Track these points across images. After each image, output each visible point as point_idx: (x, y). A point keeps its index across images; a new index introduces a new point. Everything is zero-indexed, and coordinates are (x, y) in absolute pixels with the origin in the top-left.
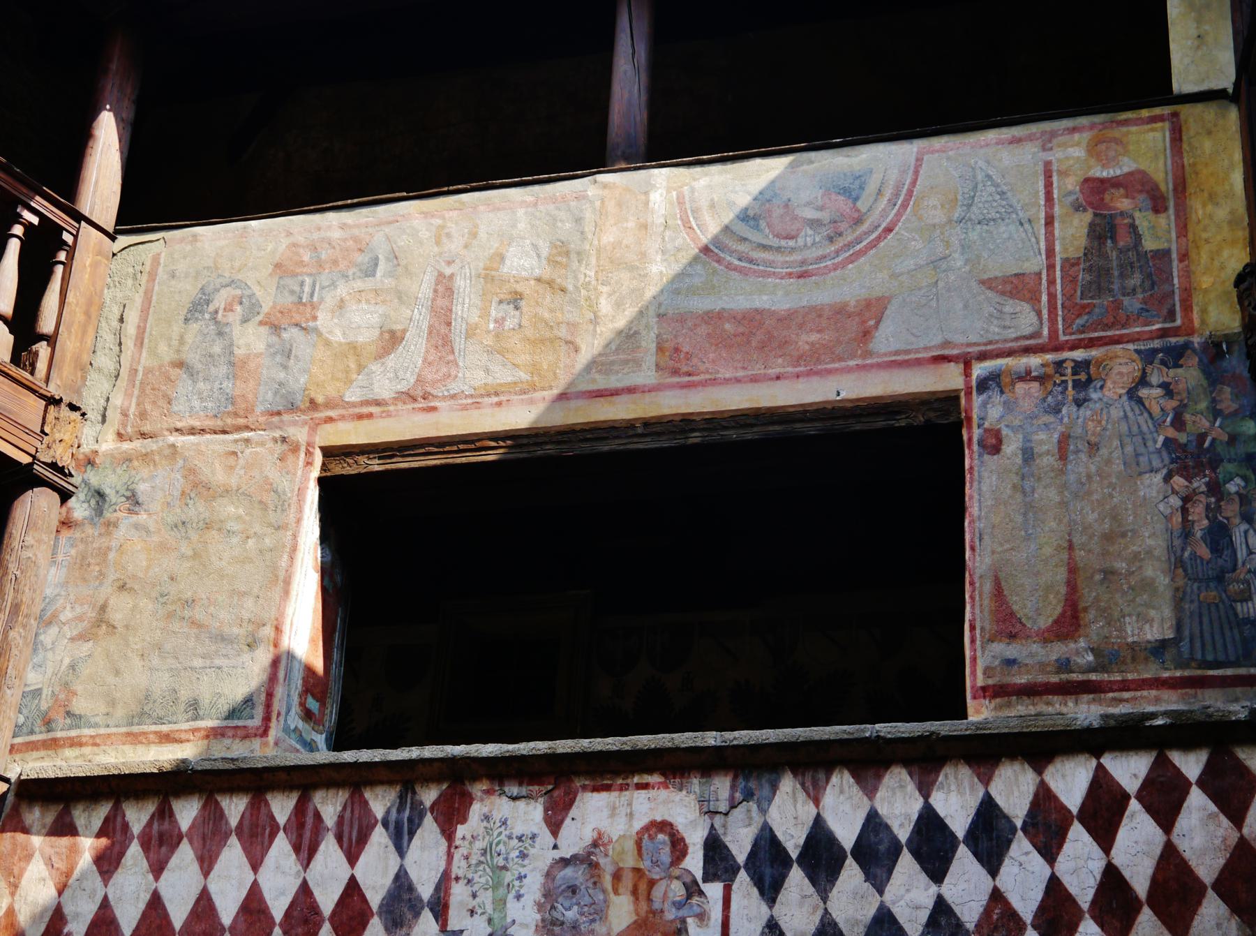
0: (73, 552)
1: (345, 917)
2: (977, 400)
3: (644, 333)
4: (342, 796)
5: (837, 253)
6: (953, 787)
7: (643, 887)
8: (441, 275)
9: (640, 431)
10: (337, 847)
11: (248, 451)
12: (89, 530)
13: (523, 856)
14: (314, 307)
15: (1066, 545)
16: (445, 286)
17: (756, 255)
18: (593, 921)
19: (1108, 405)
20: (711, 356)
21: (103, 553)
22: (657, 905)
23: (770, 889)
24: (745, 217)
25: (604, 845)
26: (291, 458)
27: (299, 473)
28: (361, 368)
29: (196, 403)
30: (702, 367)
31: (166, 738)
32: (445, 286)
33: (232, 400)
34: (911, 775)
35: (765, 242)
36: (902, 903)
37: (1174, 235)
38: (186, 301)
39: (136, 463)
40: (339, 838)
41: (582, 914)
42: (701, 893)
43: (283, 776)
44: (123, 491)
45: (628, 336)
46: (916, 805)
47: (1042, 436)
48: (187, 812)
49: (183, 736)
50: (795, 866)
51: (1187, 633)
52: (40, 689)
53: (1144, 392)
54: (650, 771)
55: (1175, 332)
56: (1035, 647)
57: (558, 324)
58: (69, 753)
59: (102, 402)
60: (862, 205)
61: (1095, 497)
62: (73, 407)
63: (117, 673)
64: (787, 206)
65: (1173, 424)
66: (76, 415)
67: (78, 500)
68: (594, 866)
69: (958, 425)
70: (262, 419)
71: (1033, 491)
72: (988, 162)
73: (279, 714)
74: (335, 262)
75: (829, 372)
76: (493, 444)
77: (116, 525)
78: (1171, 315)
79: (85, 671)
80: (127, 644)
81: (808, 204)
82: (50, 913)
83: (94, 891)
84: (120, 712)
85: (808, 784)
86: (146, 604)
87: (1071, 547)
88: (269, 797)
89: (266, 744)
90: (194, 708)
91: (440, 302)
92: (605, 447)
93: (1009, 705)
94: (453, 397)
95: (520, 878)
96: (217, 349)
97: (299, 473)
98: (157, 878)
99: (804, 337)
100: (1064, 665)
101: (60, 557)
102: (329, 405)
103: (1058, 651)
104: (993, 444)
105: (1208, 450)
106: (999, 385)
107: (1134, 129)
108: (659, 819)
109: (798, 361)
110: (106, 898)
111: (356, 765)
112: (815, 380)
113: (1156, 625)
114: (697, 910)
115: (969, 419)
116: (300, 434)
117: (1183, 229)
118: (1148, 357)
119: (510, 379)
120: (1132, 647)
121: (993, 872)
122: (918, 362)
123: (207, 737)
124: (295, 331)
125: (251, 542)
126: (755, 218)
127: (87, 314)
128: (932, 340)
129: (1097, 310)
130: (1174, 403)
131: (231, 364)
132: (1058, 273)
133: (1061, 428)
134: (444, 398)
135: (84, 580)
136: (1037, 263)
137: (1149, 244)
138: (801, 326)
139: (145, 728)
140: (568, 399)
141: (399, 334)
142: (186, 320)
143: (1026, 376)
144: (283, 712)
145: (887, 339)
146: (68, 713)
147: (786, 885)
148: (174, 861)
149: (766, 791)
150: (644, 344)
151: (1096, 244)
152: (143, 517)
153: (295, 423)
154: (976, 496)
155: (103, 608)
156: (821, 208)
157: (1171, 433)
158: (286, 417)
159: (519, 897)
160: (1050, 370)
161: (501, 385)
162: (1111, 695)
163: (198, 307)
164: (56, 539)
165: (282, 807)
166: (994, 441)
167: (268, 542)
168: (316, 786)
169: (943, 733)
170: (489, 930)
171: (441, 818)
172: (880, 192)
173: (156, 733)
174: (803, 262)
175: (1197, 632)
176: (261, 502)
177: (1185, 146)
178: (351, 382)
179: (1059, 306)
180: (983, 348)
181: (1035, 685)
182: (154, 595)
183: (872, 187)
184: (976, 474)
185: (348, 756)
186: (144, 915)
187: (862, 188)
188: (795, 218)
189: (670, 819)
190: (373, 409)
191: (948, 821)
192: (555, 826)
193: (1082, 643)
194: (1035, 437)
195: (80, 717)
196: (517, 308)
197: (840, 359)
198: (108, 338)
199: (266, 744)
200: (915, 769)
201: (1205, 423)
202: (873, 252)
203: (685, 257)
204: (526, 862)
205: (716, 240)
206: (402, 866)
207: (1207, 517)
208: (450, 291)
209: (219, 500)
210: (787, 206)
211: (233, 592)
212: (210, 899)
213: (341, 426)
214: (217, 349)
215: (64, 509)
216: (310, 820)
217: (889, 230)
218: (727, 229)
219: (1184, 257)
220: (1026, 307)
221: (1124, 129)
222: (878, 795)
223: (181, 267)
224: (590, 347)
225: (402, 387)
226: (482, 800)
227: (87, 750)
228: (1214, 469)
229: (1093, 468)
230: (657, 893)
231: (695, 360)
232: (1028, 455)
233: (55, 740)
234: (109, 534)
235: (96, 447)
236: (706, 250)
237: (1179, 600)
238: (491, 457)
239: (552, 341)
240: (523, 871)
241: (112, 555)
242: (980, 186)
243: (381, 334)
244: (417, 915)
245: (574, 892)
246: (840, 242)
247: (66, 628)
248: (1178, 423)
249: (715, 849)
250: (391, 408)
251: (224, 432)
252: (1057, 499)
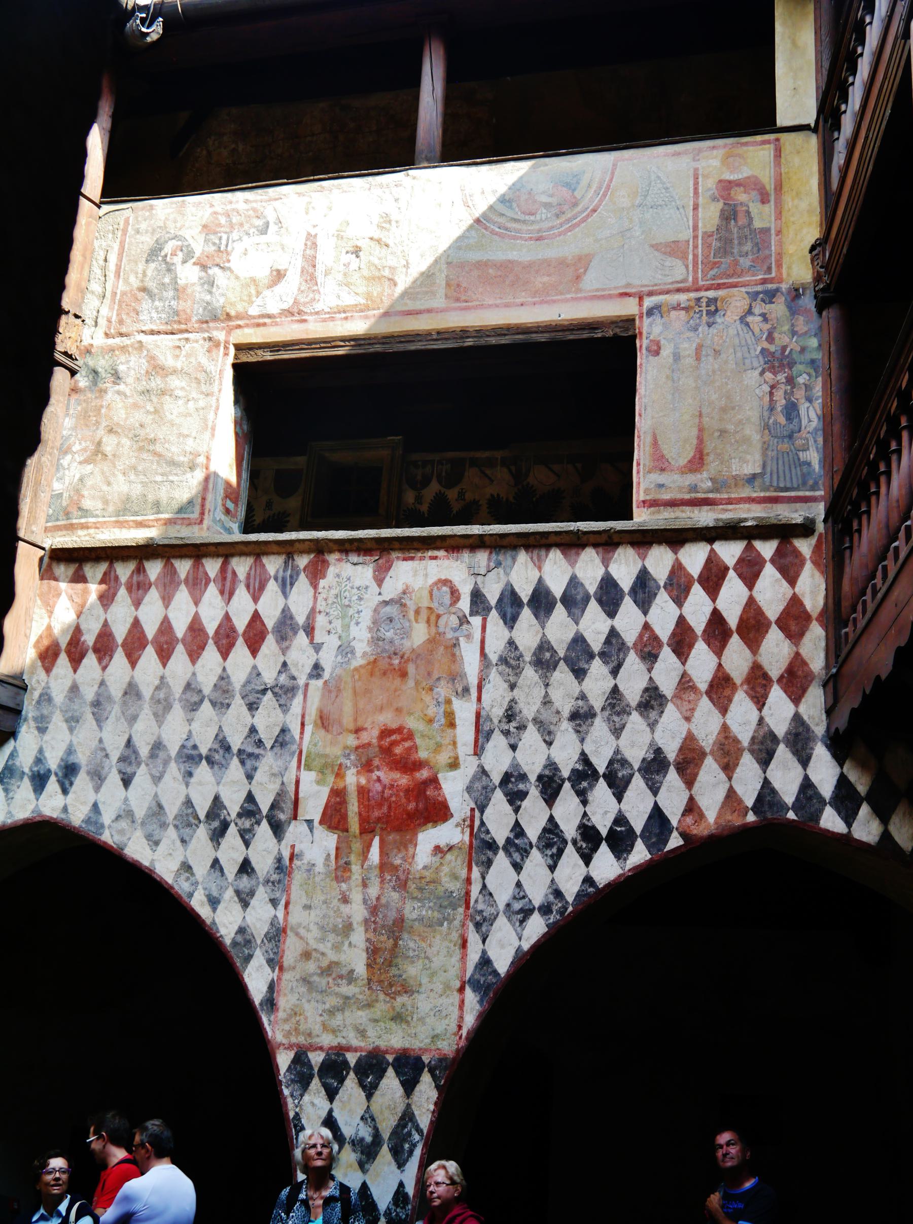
0: (79, 408)
1: (251, 634)
2: (646, 321)
3: (438, 274)
4: (249, 561)
5: (561, 225)
6: (623, 561)
7: (433, 618)
8: (309, 234)
9: (435, 337)
10: (246, 592)
11: (187, 346)
12: (89, 395)
13: (360, 599)
14: (228, 254)
15: (698, 414)
16: (312, 242)
17: (509, 225)
18: (403, 638)
19: (728, 327)
20: (480, 290)
21: (98, 409)
22: (441, 630)
23: (510, 621)
24: (503, 200)
25: (410, 593)
26: (214, 351)
27: (220, 360)
28: (258, 294)
29: (154, 315)
30: (474, 297)
31: (140, 525)
32: (312, 242)
33: (177, 313)
34: (597, 553)
35: (516, 217)
36: (590, 630)
37: (773, 218)
38: (146, 248)
39: (117, 353)
40: (248, 587)
41: (396, 634)
42: (468, 622)
43: (213, 549)
44: (109, 370)
45: (427, 277)
46: (600, 572)
47: (686, 345)
48: (154, 569)
49: (151, 523)
50: (526, 607)
51: (768, 470)
52: (62, 494)
53: (750, 319)
54: (438, 548)
55: (771, 281)
56: (677, 477)
57: (384, 267)
58: (81, 532)
59: (95, 313)
60: (578, 194)
61: (717, 384)
62: (77, 316)
63: (109, 484)
64: (530, 193)
65: (767, 339)
66: (79, 321)
67: (81, 375)
68: (404, 605)
69: (634, 337)
70: (196, 326)
71: (679, 379)
72: (658, 168)
73: (209, 511)
74: (241, 225)
75: (554, 301)
76: (342, 344)
77: (105, 391)
78: (769, 269)
79: (89, 482)
80: (115, 467)
81: (544, 192)
82: (73, 629)
83: (99, 617)
84: (111, 509)
85: (535, 558)
86: (126, 442)
87: (700, 415)
88: (204, 561)
89: (202, 529)
90: (157, 506)
91: (308, 252)
92: (412, 347)
93: (659, 512)
94: (317, 313)
95: (358, 612)
96: (167, 280)
97: (220, 360)
98: (137, 609)
99: (539, 279)
100: (694, 488)
101: (71, 412)
102: (238, 317)
103: (690, 479)
104: (656, 351)
105: (788, 356)
106: (660, 312)
107: (751, 148)
108: (443, 578)
109: (535, 293)
110: (106, 621)
111: (257, 543)
112: (545, 306)
113: (750, 464)
114: (466, 633)
115: (641, 333)
116: (220, 335)
117: (779, 215)
118: (754, 296)
119: (353, 302)
120: (735, 478)
121: (645, 613)
122: (610, 297)
123: (165, 524)
124: (216, 270)
125: (191, 404)
126: (510, 201)
127: (84, 256)
128: (619, 283)
129: (723, 266)
130: (768, 326)
131: (176, 290)
132: (700, 242)
133: (698, 341)
134: (311, 314)
135: (87, 425)
136: (688, 234)
137: (757, 224)
138: (537, 272)
139: (127, 518)
140: (390, 316)
141: (282, 272)
142: (147, 261)
143: (677, 307)
144: (212, 509)
145: (591, 281)
146: (80, 509)
147: (520, 619)
148: (147, 599)
149: (509, 560)
150: (438, 281)
151: (724, 223)
152: (122, 387)
153: (217, 329)
154: (643, 382)
155: (99, 443)
156: (551, 196)
157: (766, 345)
158: (211, 325)
159: (357, 623)
160: (692, 304)
161: (347, 306)
162: (721, 507)
163: (154, 253)
164: (69, 400)
165: (212, 567)
166: (656, 348)
167: (201, 404)
168: (233, 555)
169: (618, 529)
170: (339, 643)
171: (310, 576)
172: (589, 186)
173: (133, 521)
174: (539, 231)
175: (775, 470)
176: (196, 378)
177: (783, 160)
178: (252, 302)
179: (700, 263)
180: (651, 288)
181: (675, 500)
182: (130, 436)
183: (584, 182)
184: (644, 368)
185: (253, 537)
186: (130, 632)
187: (578, 183)
188: (535, 201)
189: (450, 578)
190: (267, 320)
191: (618, 582)
192: (380, 582)
193: (705, 475)
194: (682, 346)
195: (87, 511)
196: (357, 257)
197: (561, 294)
198: (98, 272)
199: (202, 529)
200: (600, 550)
201: (786, 340)
202: (583, 225)
203: (464, 226)
204: (362, 603)
205: (484, 215)
206: (286, 604)
207: (785, 398)
208: (315, 245)
209: (170, 377)
210: (530, 193)
211: (180, 435)
212: (169, 622)
213: (247, 331)
214: (167, 280)
215: (73, 381)
216: (229, 575)
217: (594, 211)
218: (491, 208)
219: (779, 233)
220: (678, 263)
221: (745, 148)
222: (577, 565)
223: (143, 226)
224: (404, 282)
225: (285, 306)
226: (335, 565)
227: (92, 531)
228: (790, 368)
229: (716, 366)
230: (442, 622)
231: (470, 293)
232: (677, 357)
233: (72, 525)
234: (102, 397)
235: (91, 342)
236: (478, 221)
237: (765, 449)
238: (341, 352)
239: (379, 278)
240: (360, 608)
241: (103, 411)
242: (653, 183)
243: (272, 271)
244: (295, 633)
245: (391, 621)
246: (563, 218)
247: (76, 456)
248: (770, 338)
249: (477, 597)
250: (278, 320)
251: (172, 333)
252: (694, 385)
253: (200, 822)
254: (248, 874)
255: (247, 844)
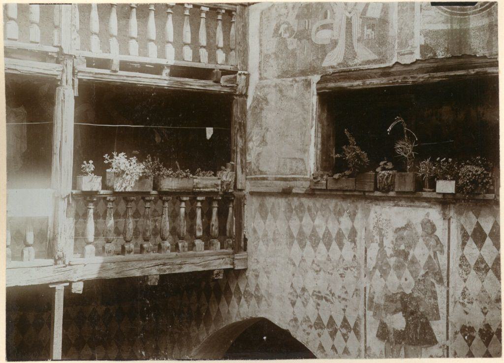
95: (387, 232)
155: (263, 137)
245: (403, 239)
253: (325, 327)
254: (347, 353)
255: (346, 341)
